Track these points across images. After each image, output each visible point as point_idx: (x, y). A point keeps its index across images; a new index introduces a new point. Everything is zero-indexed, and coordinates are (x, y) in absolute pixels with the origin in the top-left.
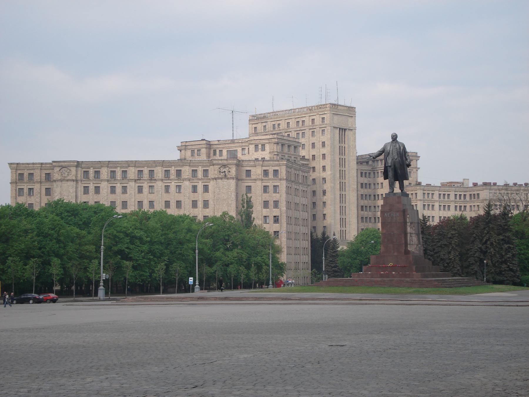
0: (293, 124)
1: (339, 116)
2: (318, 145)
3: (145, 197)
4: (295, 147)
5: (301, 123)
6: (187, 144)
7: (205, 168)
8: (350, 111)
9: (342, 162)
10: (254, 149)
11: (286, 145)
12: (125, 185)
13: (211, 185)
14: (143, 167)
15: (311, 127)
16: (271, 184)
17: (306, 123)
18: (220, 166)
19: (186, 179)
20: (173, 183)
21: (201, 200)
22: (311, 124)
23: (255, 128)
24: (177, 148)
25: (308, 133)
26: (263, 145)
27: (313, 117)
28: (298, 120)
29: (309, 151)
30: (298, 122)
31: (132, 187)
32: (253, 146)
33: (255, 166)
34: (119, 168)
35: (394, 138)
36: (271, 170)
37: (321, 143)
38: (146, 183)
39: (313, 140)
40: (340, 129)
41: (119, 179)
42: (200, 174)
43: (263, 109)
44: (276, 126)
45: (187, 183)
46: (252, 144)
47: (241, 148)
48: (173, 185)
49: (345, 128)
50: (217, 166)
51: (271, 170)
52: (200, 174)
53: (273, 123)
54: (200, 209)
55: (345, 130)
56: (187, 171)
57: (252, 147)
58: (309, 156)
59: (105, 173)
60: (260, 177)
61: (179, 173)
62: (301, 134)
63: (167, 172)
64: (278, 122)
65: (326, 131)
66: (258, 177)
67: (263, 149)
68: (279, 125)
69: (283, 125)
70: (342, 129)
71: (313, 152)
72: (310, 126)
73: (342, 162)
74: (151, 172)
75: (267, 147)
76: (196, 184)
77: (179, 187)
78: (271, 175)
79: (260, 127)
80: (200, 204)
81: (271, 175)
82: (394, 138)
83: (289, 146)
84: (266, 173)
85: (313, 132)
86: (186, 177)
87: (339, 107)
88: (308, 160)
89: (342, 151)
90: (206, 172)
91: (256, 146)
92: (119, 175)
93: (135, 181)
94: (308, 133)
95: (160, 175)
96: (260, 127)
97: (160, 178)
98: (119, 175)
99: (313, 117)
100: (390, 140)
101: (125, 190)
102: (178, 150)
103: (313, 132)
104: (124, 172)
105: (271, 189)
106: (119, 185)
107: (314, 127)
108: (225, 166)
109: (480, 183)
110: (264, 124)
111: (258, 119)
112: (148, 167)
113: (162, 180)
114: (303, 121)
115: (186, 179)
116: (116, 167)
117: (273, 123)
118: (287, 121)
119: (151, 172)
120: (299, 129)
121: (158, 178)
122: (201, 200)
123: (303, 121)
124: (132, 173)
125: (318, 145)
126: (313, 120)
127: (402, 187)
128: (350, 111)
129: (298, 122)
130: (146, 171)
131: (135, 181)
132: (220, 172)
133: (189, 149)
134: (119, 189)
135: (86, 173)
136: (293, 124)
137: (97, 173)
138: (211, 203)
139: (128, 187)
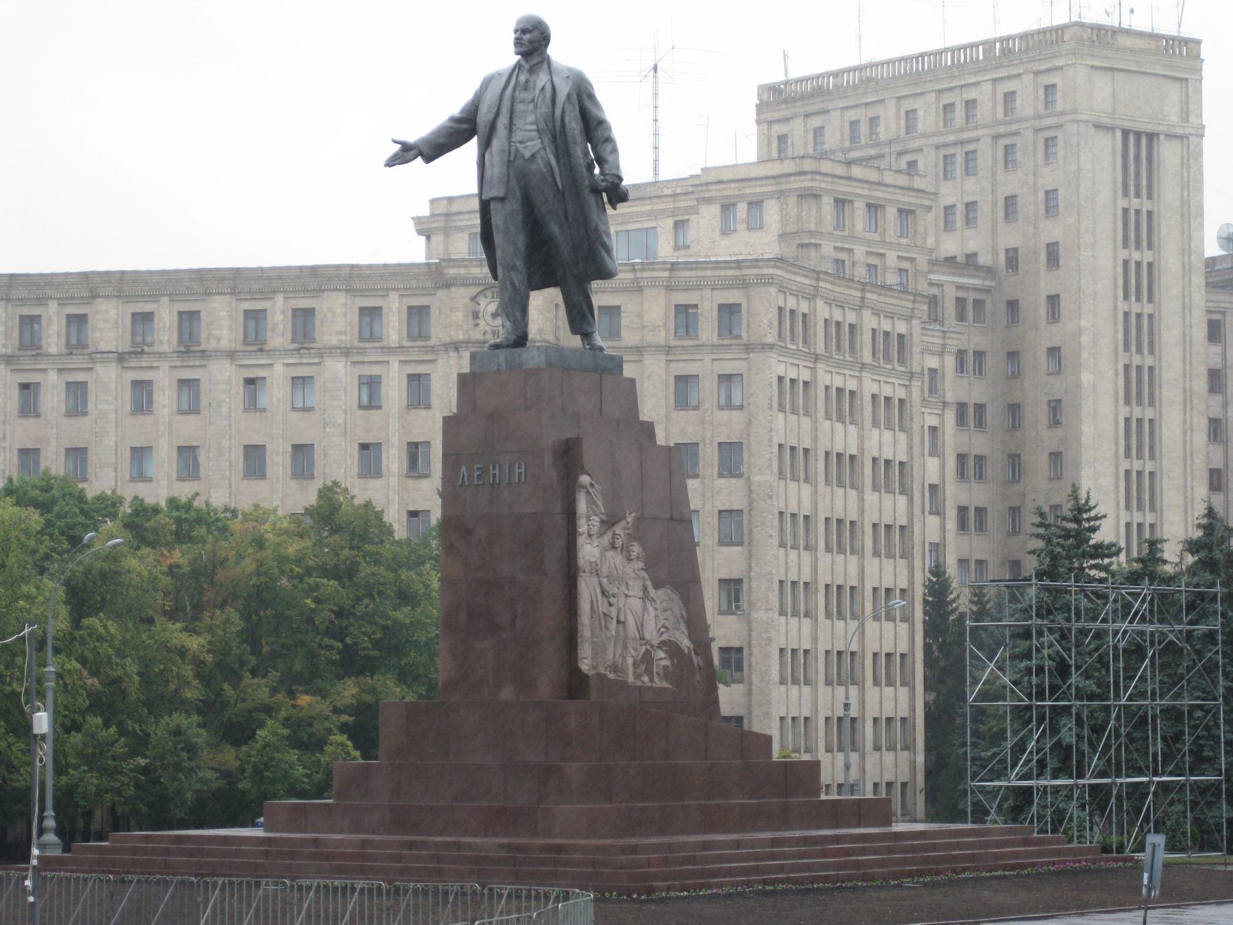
0: (928, 120)
1: (1120, 77)
3: (165, 427)
4: (905, 213)
5: (959, 111)
6: (456, 207)
7: (416, 302)
8: (1177, 58)
9: (1139, 281)
10: (717, 223)
11: (860, 205)
12: (79, 377)
14: (155, 298)
15: (1002, 130)
16: (706, 368)
17: (983, 113)
18: (474, 290)
19: (330, 351)
20: (278, 368)
21: (395, 440)
22: (1000, 115)
23: (782, 139)
24: (411, 227)
25: (987, 153)
26: (755, 204)
27: (1011, 86)
28: (947, 99)
29: (994, 230)
30: (949, 108)
31: (109, 385)
32: (715, 210)
33: (640, 290)
34: (53, 306)
35: (533, 41)
36: (708, 304)
37: (1041, 196)
38: (165, 366)
39: (1010, 184)
40: (1126, 133)
41: (53, 350)
42: (394, 328)
44: (864, 129)
45: (337, 368)
46: (709, 201)
47: (669, 222)
48: (278, 375)
49: (1151, 128)
50: (462, 291)
51: (708, 304)
52: (394, 328)
53: (851, 115)
54: (394, 482)
55: (1151, 136)
58: (995, 254)
60: (661, 337)
61: (304, 319)
62: (959, 159)
63: (255, 318)
64: (872, 112)
65: (1060, 143)
66: (650, 338)
67: (755, 225)
68: (874, 121)
69: (890, 124)
70: (1138, 135)
71: (1010, 237)
72: (996, 123)
73: (1139, 281)
74: (189, 319)
75: (772, 212)
76: (375, 370)
77: (301, 382)
78: (708, 330)
79: (798, 131)
81: (708, 330)
82: (533, 41)
83: (874, 208)
84: (685, 316)
85: (1009, 149)
86: (334, 341)
87: (1123, 41)
88: (990, 271)
89: (1138, 229)
90: (418, 316)
91: (727, 208)
92: (53, 337)
93: (121, 358)
94: (987, 153)
95: (225, 333)
96: (798, 131)
97: (225, 344)
98: (53, 337)
99: (1011, 86)
100: (509, 58)
101: (77, 397)
102: (420, 232)
103: (1009, 149)
104: (77, 321)
105: (708, 389)
106: (52, 377)
107: (1014, 128)
110: (816, 122)
111: (791, 100)
112: (173, 297)
113: (231, 355)
114: (970, 105)
115: (330, 351)
116: (42, 301)
117: (851, 115)
118: (907, 105)
119: (189, 319)
120: (951, 138)
121: (213, 345)
122: (395, 440)
123: (970, 105)
124: (109, 324)
125: (1030, 204)
126: (1010, 96)
127: (580, 316)
128: (1177, 58)
129: (949, 108)
130: (166, 316)
131: (121, 358)
132: (476, 315)
133: (461, 229)
134: (53, 398)
136: (928, 120)
139: (91, 386)
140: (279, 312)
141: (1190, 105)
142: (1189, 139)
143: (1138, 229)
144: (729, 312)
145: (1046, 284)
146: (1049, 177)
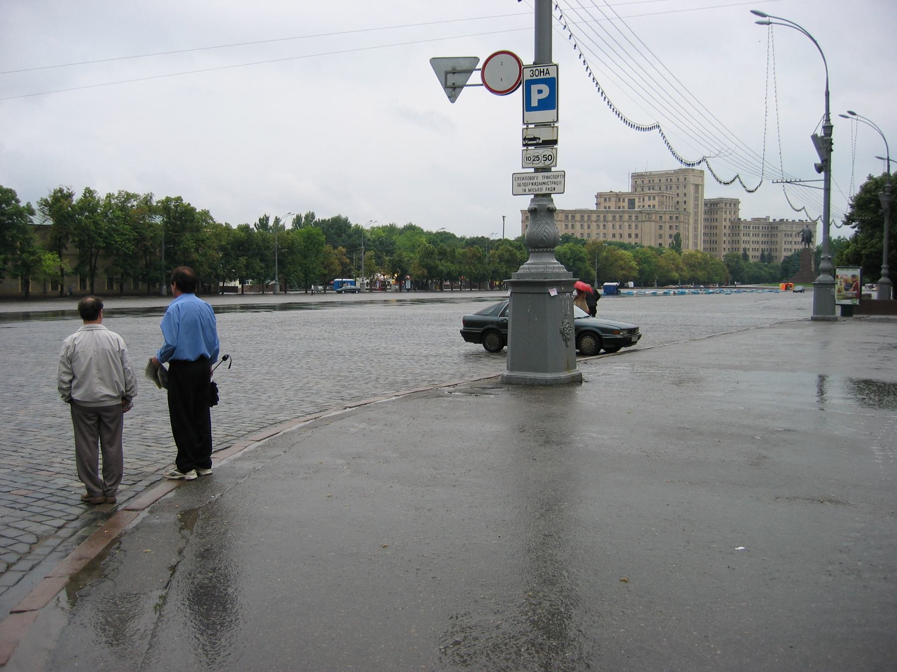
2: (681, 195)
9: (696, 206)
13: (640, 225)
16: (674, 225)
25: (674, 187)
26: (654, 198)
31: (594, 226)
39: (678, 191)
42: (633, 219)
43: (641, 170)
52: (633, 219)
56: (626, 217)
57: (646, 198)
59: (578, 217)
67: (654, 199)
73: (696, 206)
75: (657, 198)
79: (639, 181)
80: (633, 236)
84: (671, 218)
89: (696, 199)
90: (637, 217)
94: (674, 187)
108: (649, 214)
109: (778, 220)
125: (681, 195)
135: (567, 217)
137: (573, 217)
138: (639, 235)
140: (617, 216)
141: (703, 181)
142: (702, 186)
143: (696, 199)
144: (677, 217)
145: (684, 206)
146: (685, 191)
